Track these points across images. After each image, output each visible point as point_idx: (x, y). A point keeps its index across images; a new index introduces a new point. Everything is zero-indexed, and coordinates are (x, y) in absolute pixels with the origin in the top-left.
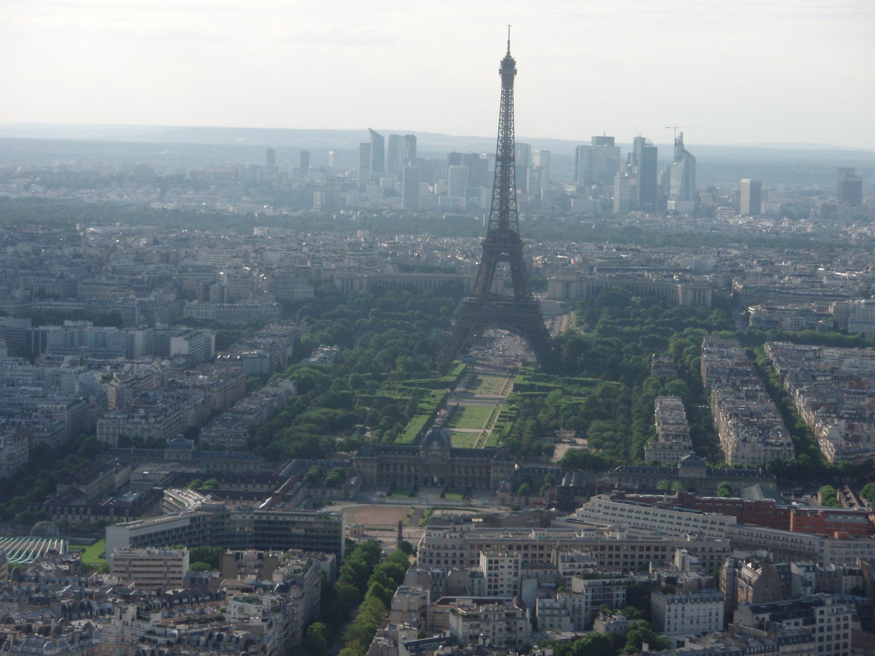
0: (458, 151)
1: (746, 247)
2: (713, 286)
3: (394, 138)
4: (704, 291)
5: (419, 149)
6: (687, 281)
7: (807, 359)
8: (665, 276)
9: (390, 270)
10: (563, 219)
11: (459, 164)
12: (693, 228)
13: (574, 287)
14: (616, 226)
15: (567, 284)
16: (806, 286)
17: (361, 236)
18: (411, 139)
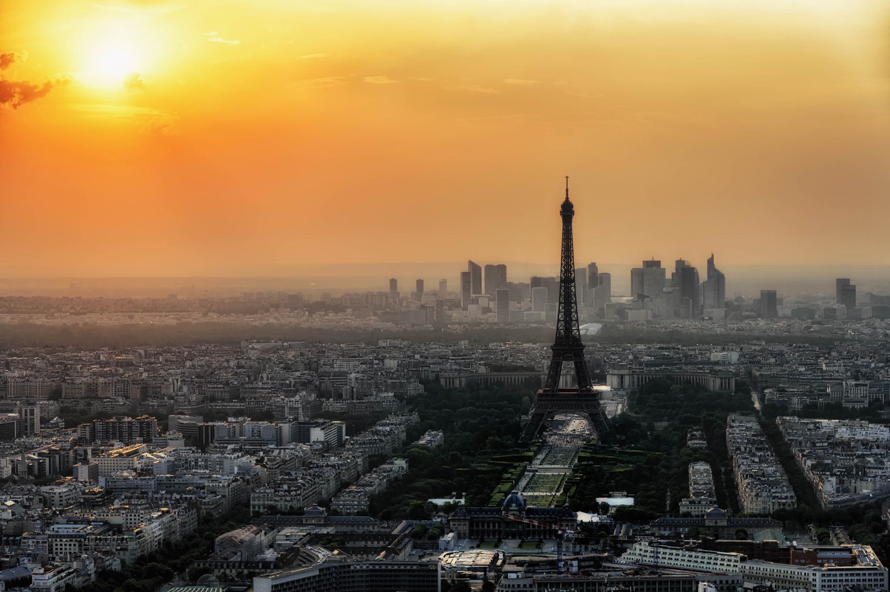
0: (538, 276)
1: (764, 343)
2: (737, 374)
3: (489, 268)
4: (729, 379)
5: (508, 276)
6: (715, 373)
7: (809, 430)
8: (699, 369)
9: (482, 370)
10: (621, 327)
11: (540, 286)
12: (723, 330)
13: (627, 380)
14: (663, 330)
15: (622, 377)
16: (809, 372)
17: (463, 344)
18: (502, 269)
